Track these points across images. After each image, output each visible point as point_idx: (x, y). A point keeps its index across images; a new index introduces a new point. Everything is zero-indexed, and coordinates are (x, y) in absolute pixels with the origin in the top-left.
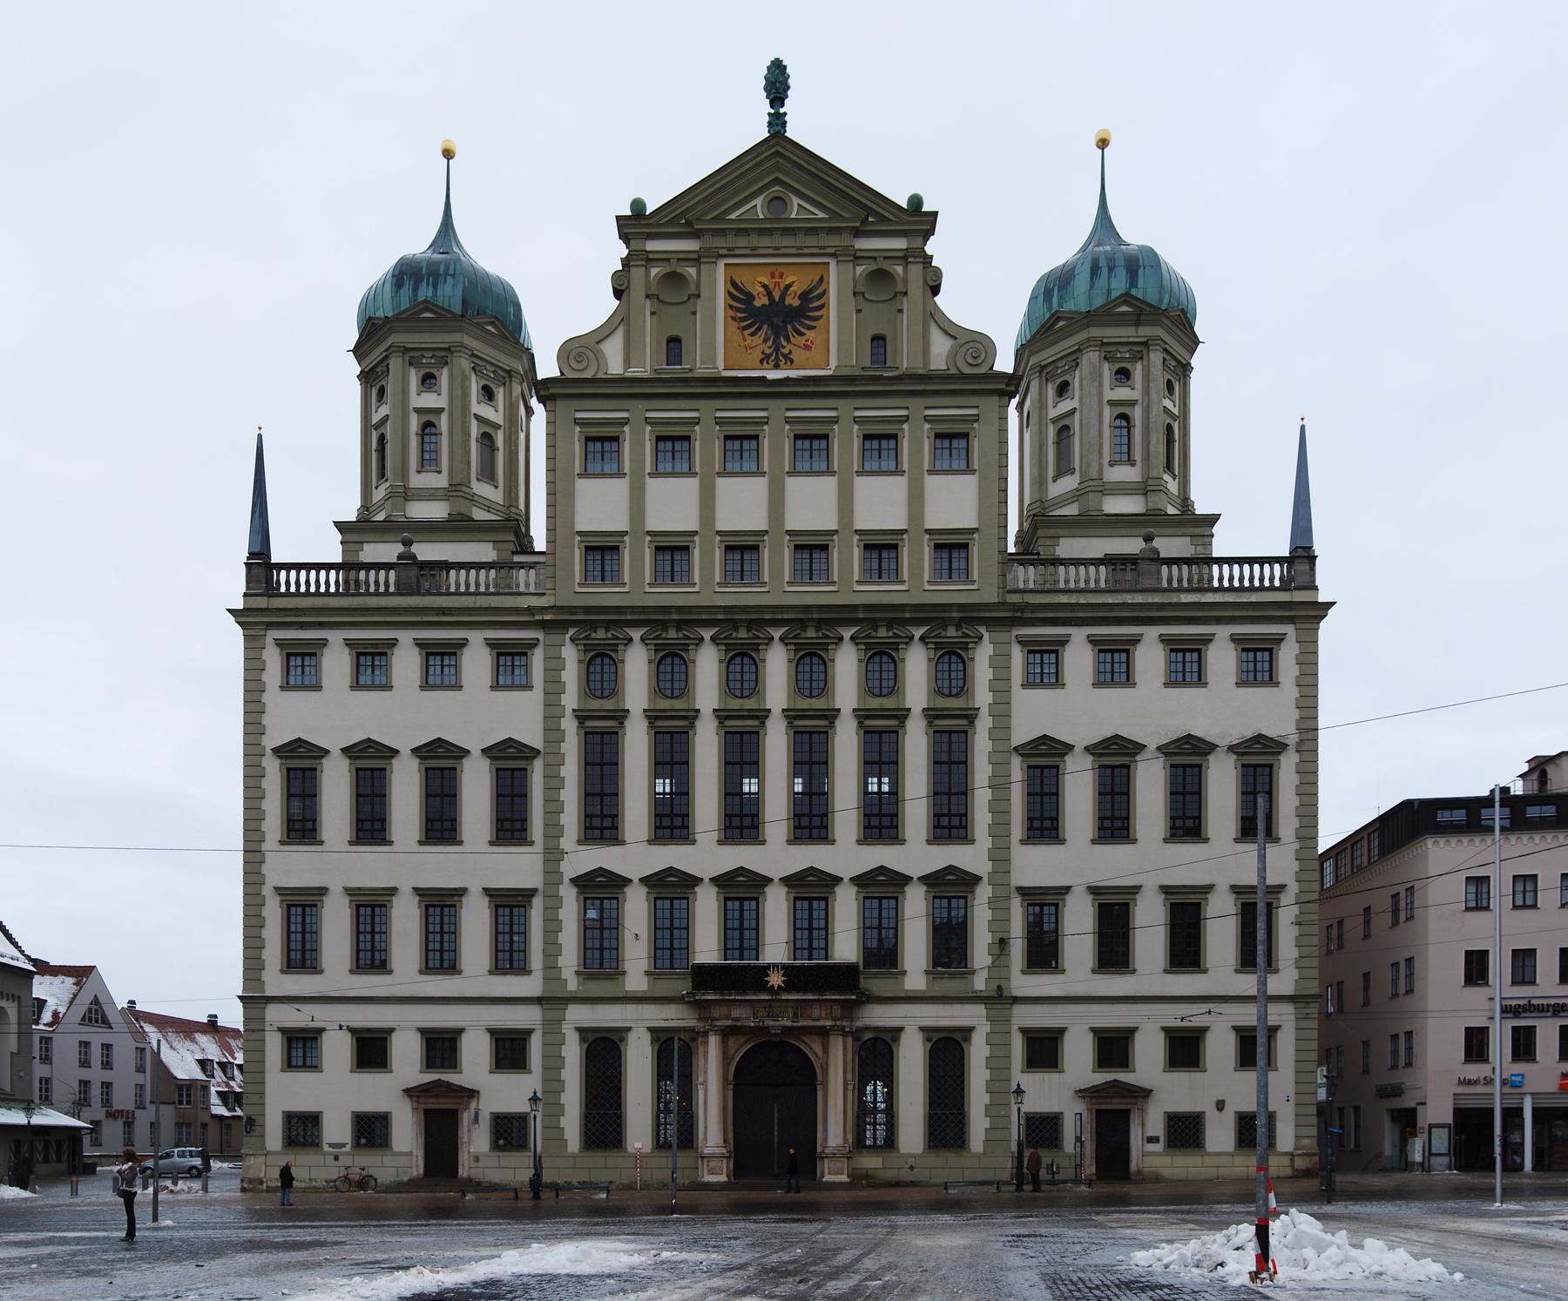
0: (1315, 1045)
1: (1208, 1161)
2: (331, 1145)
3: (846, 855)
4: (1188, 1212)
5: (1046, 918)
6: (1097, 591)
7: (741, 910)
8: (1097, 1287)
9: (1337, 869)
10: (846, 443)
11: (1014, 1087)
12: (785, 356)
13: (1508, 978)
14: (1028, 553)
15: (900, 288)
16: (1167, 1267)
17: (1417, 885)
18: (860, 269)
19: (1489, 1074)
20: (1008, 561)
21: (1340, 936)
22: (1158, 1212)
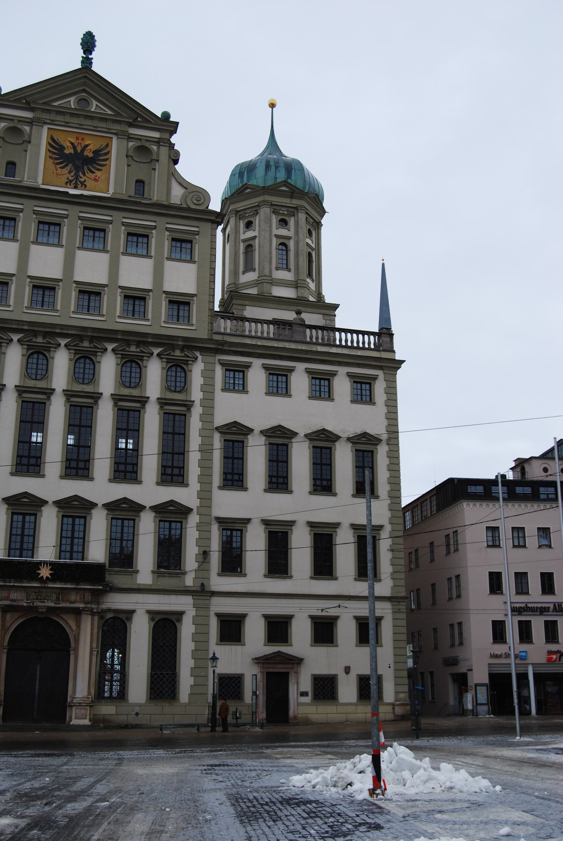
0: (404, 630)
1: (341, 709)
3: (100, 488)
4: (328, 746)
5: (234, 539)
6: (268, 339)
7: (24, 522)
8: (267, 804)
9: (413, 517)
10: (117, 235)
11: (211, 655)
12: (81, 182)
13: (514, 591)
14: (227, 312)
15: (154, 157)
16: (314, 787)
17: (459, 530)
18: (131, 144)
19: (507, 651)
20: (214, 315)
21: (417, 559)
22: (308, 746)
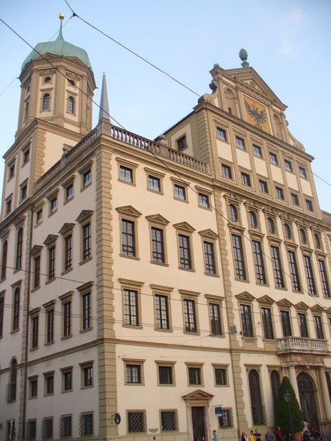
2: (151, 430)
